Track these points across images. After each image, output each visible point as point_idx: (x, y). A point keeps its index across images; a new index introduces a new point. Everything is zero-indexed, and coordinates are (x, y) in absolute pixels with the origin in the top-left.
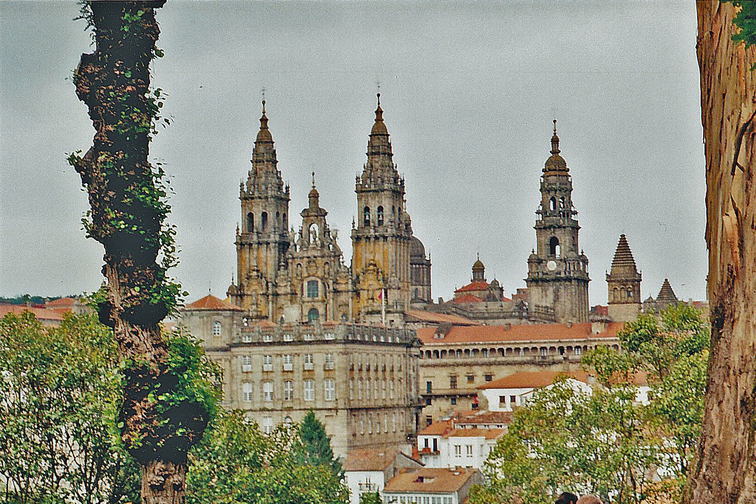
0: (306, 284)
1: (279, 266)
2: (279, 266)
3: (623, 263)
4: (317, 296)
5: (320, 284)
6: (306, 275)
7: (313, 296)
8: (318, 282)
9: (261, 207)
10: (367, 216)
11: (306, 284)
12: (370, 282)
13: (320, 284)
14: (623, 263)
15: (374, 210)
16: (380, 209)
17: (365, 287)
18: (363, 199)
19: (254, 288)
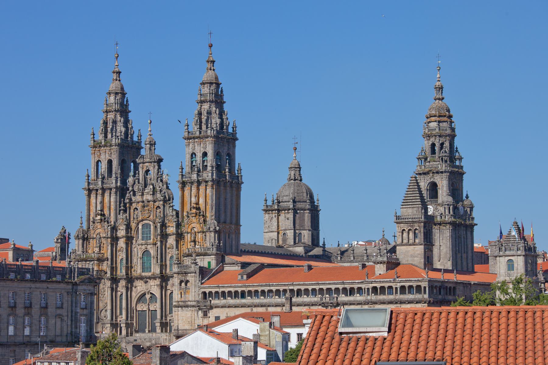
0: (140, 227)
1: (120, 211)
2: (120, 211)
3: (412, 205)
4: (150, 239)
5: (152, 227)
6: (140, 219)
7: (147, 239)
8: (150, 225)
9: (107, 155)
10: (194, 162)
11: (140, 227)
12: (193, 225)
13: (152, 227)
14: (412, 205)
15: (199, 155)
16: (205, 154)
17: (189, 230)
18: (191, 145)
19: (98, 231)
